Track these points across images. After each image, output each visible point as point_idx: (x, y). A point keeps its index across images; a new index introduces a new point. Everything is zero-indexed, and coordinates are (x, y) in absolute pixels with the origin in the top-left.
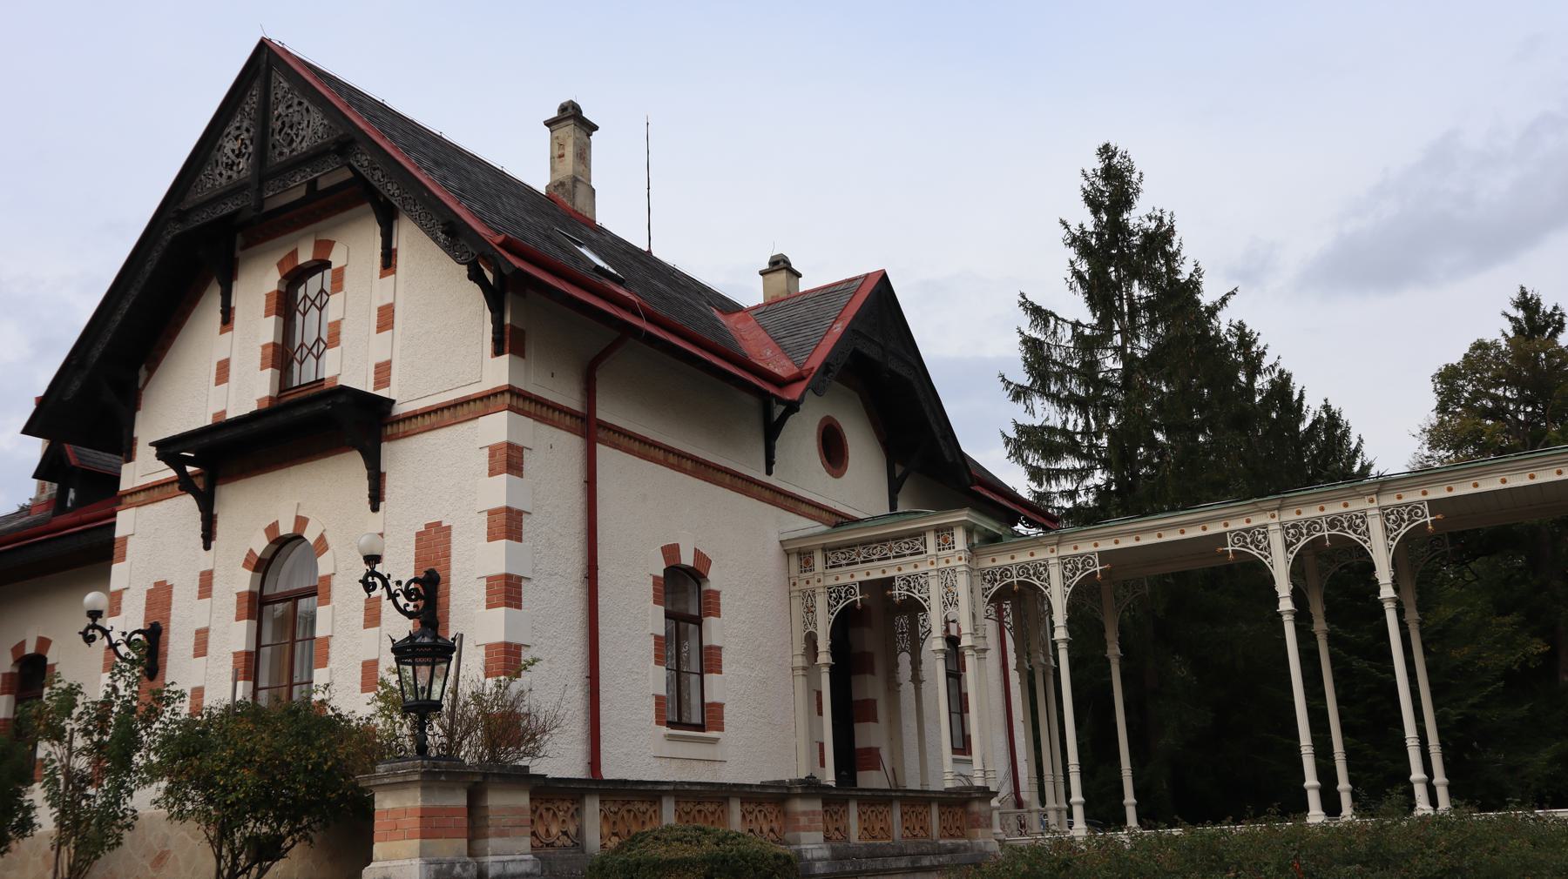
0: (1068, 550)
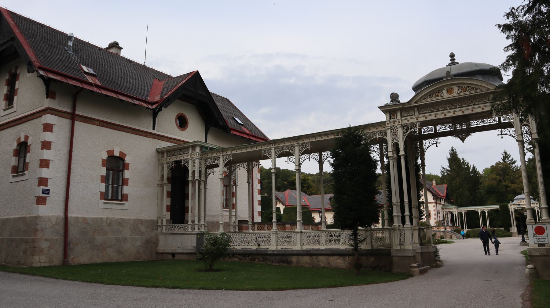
0: (464, 210)
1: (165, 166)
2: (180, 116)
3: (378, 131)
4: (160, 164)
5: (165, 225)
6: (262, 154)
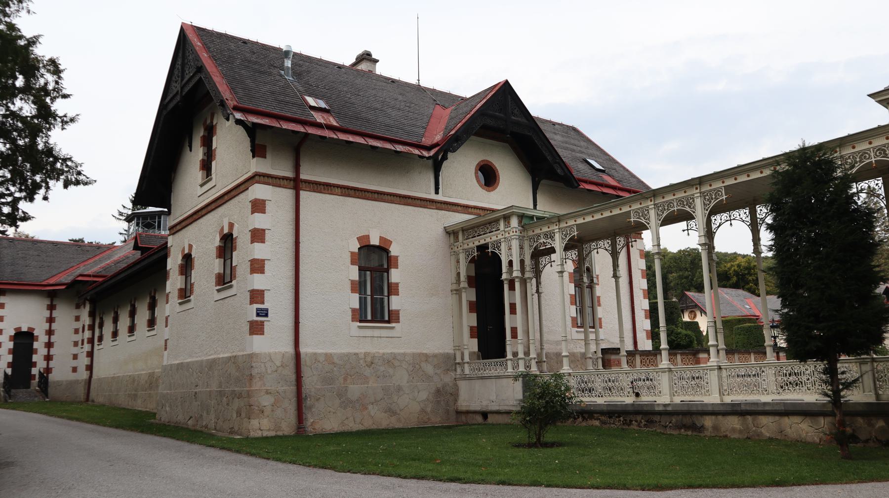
1: (462, 257)
2: (484, 165)
3: (874, 148)
4: (453, 253)
5: (468, 363)
6: (632, 220)
